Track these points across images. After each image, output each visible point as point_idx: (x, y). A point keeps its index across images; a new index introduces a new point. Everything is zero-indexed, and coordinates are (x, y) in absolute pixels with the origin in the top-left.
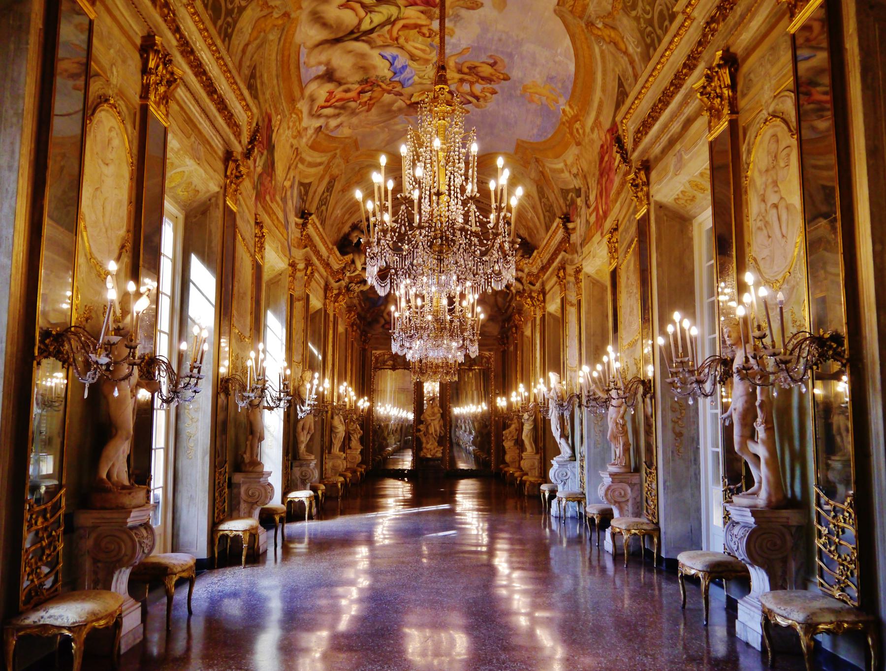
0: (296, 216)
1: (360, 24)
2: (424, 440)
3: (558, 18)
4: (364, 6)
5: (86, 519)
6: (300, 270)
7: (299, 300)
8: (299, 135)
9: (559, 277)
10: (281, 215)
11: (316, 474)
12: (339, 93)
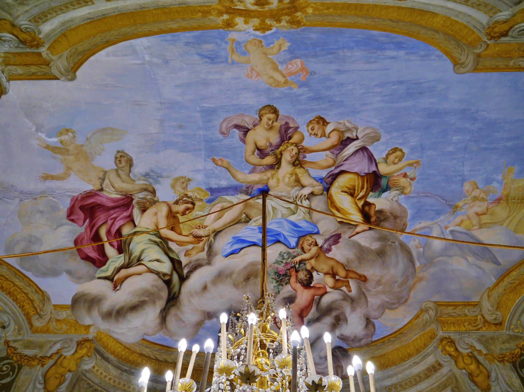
1: (157, 273)
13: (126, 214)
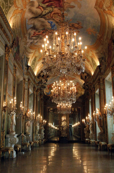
0: (25, 66)
1: (42, 13)
2: (62, 132)
3: (95, 9)
4: (43, 8)
6: (26, 81)
7: (26, 89)
8: (26, 44)
9: (98, 83)
10: (21, 65)
11: (31, 138)
12: (37, 33)
13: (58, 6)
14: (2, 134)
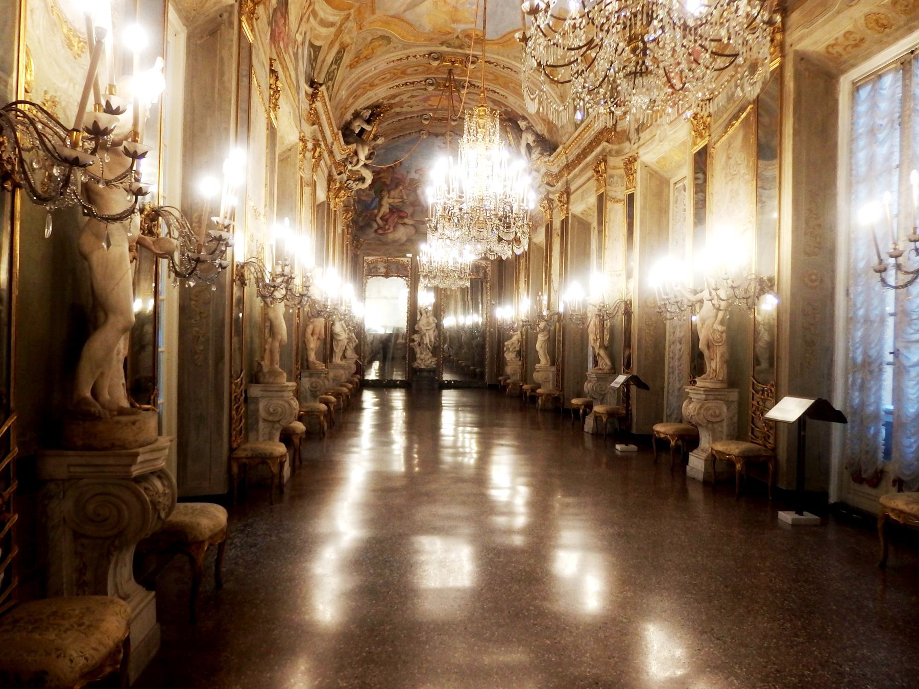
0: (306, 83)
2: (418, 350)
5: (58, 465)
10: (293, 73)
14: (234, 387)
